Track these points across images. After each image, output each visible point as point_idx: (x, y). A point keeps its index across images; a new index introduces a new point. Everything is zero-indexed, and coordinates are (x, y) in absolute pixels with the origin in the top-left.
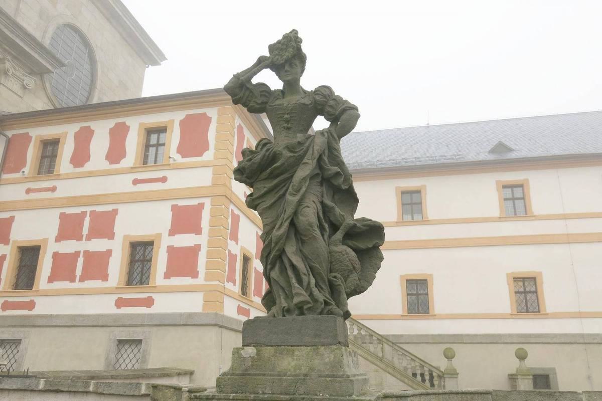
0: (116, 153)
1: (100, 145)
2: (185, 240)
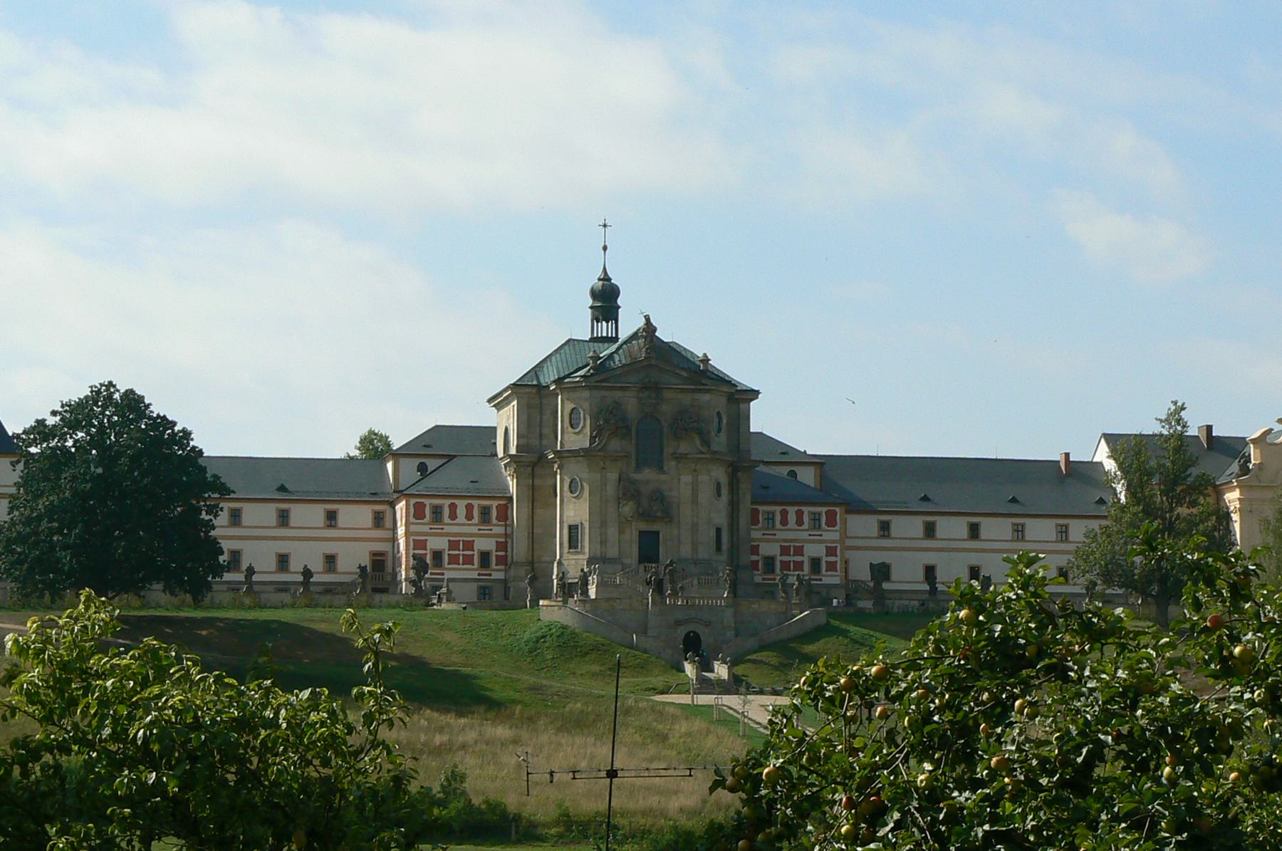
0: (800, 522)
1: (792, 518)
2: (832, 559)
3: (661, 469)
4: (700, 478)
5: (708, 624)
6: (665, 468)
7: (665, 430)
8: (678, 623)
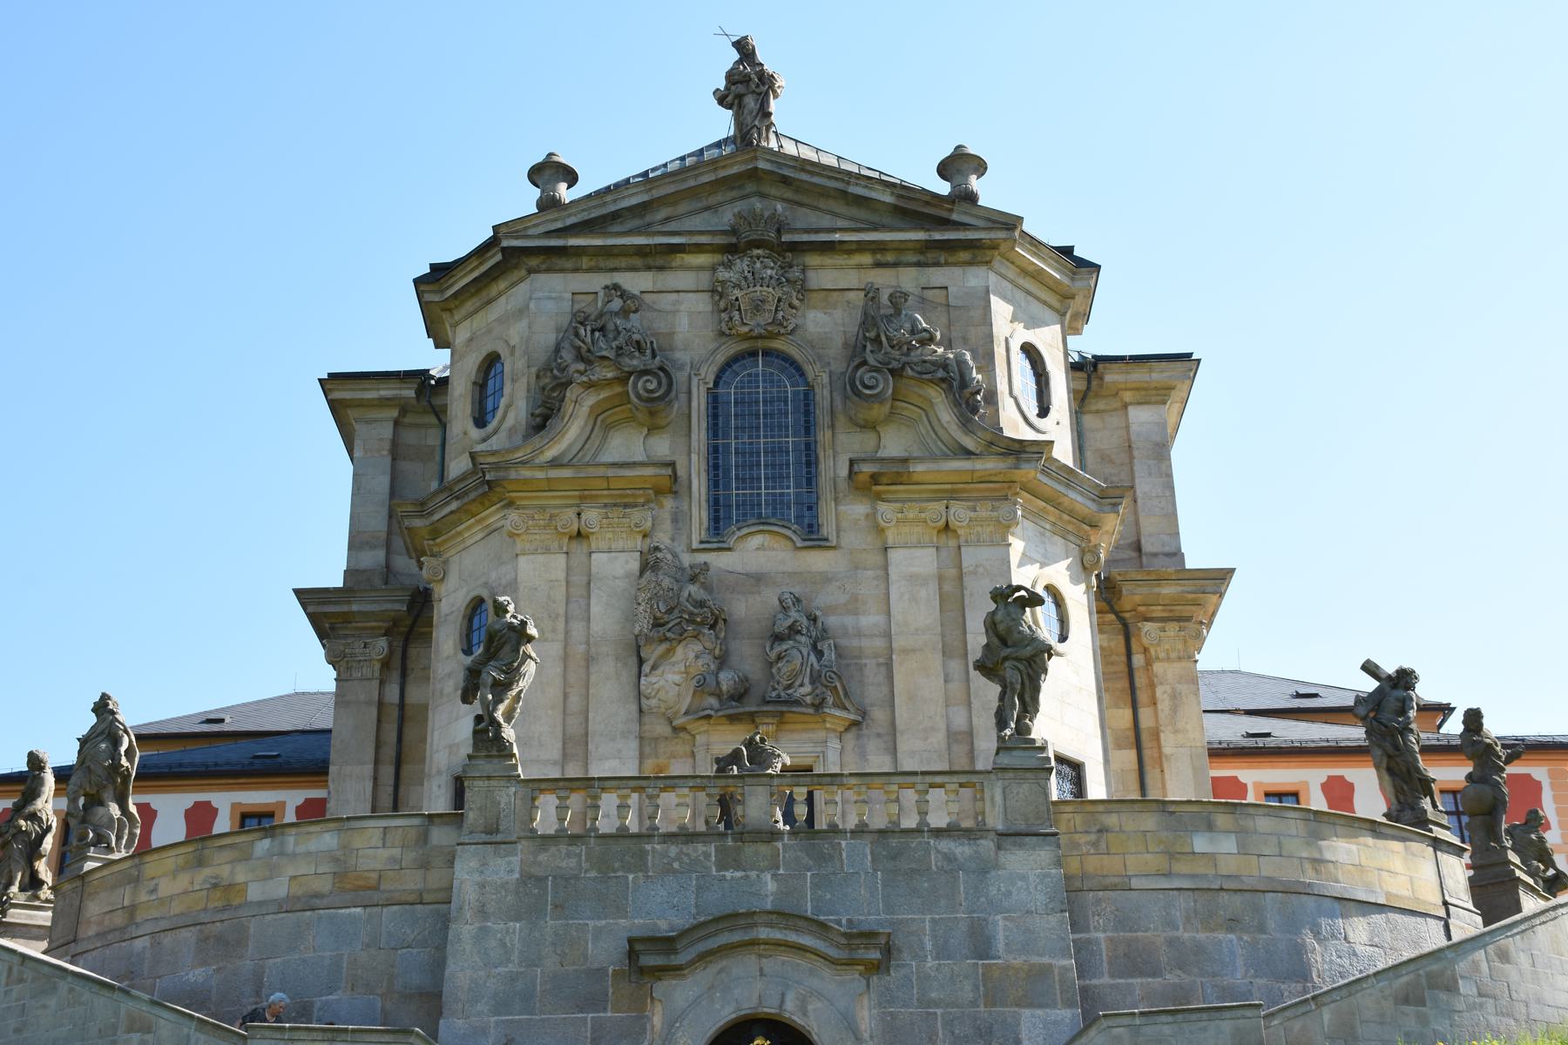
3: (812, 535)
4: (970, 557)
5: (870, 952)
6: (828, 529)
7: (823, 396)
8: (650, 960)
